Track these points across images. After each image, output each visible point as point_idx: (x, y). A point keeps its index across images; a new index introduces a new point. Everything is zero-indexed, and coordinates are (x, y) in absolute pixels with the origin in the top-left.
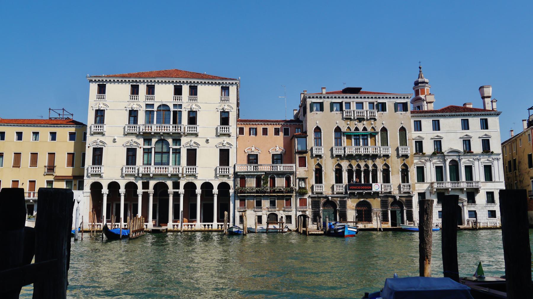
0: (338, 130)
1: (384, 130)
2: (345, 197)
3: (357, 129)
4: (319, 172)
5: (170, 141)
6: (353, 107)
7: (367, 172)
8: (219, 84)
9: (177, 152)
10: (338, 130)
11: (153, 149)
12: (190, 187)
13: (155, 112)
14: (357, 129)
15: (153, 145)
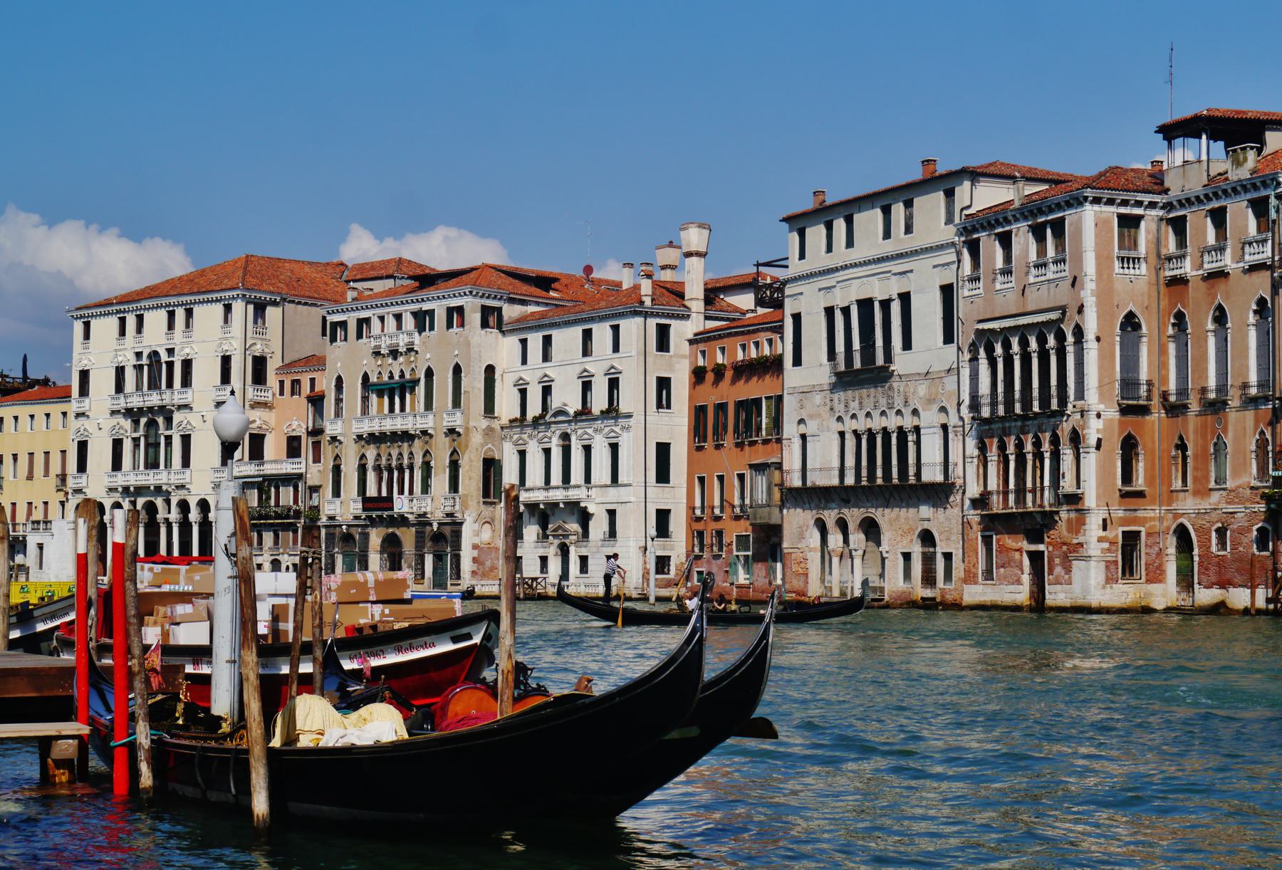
0: (366, 377)
1: (429, 373)
2: (367, 526)
3: (391, 377)
4: (337, 470)
5: (160, 420)
6: (391, 323)
7: (401, 469)
8: (217, 301)
9: (169, 439)
10: (366, 377)
11: (142, 440)
12: (184, 506)
13: (146, 368)
14: (391, 377)
15: (141, 431)
